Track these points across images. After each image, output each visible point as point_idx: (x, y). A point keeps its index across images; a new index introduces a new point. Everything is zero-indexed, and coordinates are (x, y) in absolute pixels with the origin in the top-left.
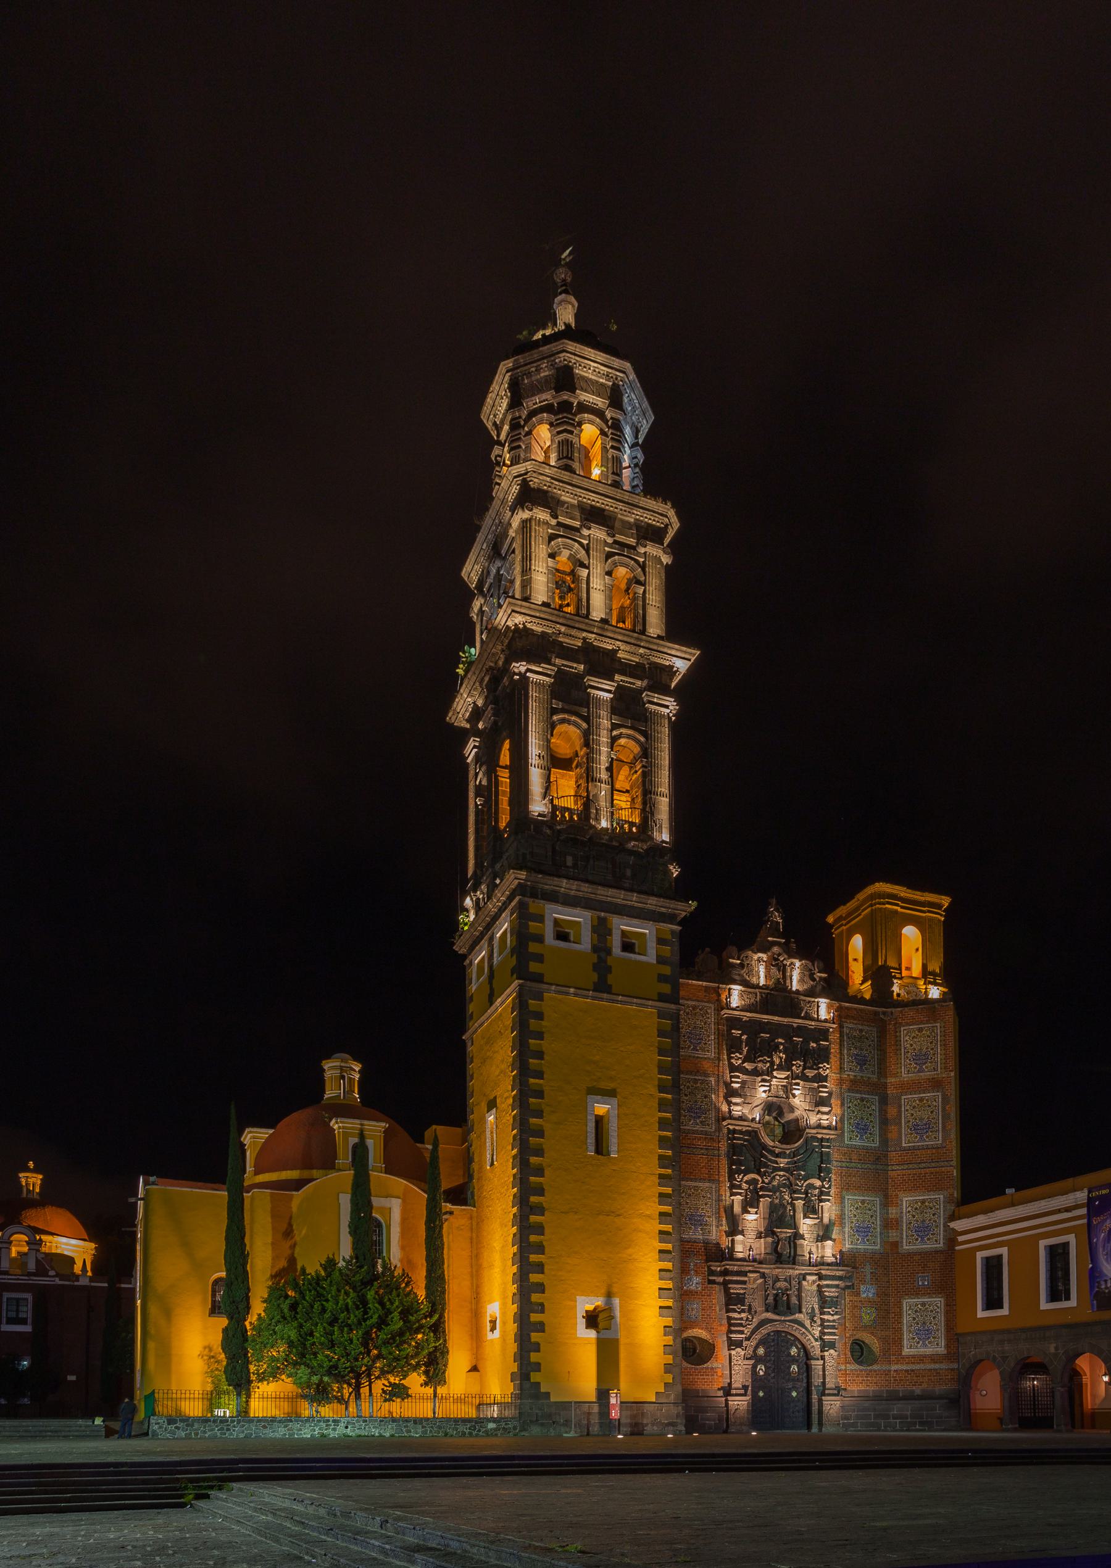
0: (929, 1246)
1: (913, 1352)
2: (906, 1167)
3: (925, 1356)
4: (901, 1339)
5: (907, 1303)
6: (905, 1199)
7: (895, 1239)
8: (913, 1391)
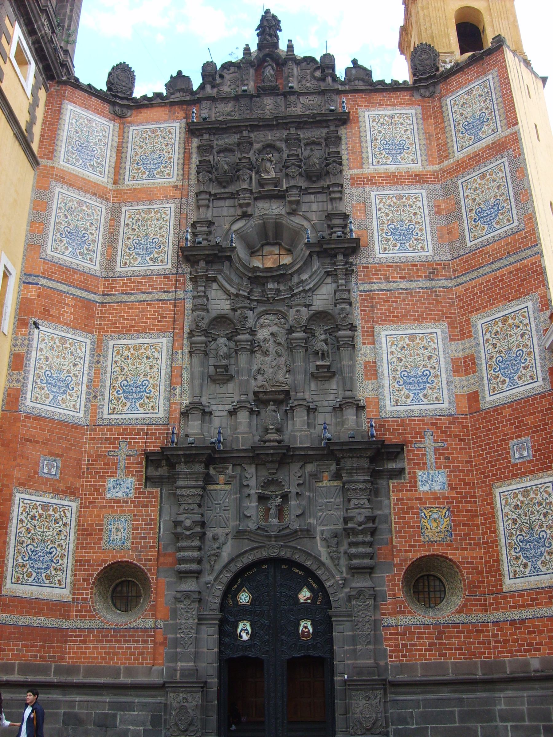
0: (522, 389)
1: (520, 584)
2: (475, 274)
3: (539, 591)
4: (498, 561)
6: (479, 323)
7: (473, 389)
8: (527, 664)
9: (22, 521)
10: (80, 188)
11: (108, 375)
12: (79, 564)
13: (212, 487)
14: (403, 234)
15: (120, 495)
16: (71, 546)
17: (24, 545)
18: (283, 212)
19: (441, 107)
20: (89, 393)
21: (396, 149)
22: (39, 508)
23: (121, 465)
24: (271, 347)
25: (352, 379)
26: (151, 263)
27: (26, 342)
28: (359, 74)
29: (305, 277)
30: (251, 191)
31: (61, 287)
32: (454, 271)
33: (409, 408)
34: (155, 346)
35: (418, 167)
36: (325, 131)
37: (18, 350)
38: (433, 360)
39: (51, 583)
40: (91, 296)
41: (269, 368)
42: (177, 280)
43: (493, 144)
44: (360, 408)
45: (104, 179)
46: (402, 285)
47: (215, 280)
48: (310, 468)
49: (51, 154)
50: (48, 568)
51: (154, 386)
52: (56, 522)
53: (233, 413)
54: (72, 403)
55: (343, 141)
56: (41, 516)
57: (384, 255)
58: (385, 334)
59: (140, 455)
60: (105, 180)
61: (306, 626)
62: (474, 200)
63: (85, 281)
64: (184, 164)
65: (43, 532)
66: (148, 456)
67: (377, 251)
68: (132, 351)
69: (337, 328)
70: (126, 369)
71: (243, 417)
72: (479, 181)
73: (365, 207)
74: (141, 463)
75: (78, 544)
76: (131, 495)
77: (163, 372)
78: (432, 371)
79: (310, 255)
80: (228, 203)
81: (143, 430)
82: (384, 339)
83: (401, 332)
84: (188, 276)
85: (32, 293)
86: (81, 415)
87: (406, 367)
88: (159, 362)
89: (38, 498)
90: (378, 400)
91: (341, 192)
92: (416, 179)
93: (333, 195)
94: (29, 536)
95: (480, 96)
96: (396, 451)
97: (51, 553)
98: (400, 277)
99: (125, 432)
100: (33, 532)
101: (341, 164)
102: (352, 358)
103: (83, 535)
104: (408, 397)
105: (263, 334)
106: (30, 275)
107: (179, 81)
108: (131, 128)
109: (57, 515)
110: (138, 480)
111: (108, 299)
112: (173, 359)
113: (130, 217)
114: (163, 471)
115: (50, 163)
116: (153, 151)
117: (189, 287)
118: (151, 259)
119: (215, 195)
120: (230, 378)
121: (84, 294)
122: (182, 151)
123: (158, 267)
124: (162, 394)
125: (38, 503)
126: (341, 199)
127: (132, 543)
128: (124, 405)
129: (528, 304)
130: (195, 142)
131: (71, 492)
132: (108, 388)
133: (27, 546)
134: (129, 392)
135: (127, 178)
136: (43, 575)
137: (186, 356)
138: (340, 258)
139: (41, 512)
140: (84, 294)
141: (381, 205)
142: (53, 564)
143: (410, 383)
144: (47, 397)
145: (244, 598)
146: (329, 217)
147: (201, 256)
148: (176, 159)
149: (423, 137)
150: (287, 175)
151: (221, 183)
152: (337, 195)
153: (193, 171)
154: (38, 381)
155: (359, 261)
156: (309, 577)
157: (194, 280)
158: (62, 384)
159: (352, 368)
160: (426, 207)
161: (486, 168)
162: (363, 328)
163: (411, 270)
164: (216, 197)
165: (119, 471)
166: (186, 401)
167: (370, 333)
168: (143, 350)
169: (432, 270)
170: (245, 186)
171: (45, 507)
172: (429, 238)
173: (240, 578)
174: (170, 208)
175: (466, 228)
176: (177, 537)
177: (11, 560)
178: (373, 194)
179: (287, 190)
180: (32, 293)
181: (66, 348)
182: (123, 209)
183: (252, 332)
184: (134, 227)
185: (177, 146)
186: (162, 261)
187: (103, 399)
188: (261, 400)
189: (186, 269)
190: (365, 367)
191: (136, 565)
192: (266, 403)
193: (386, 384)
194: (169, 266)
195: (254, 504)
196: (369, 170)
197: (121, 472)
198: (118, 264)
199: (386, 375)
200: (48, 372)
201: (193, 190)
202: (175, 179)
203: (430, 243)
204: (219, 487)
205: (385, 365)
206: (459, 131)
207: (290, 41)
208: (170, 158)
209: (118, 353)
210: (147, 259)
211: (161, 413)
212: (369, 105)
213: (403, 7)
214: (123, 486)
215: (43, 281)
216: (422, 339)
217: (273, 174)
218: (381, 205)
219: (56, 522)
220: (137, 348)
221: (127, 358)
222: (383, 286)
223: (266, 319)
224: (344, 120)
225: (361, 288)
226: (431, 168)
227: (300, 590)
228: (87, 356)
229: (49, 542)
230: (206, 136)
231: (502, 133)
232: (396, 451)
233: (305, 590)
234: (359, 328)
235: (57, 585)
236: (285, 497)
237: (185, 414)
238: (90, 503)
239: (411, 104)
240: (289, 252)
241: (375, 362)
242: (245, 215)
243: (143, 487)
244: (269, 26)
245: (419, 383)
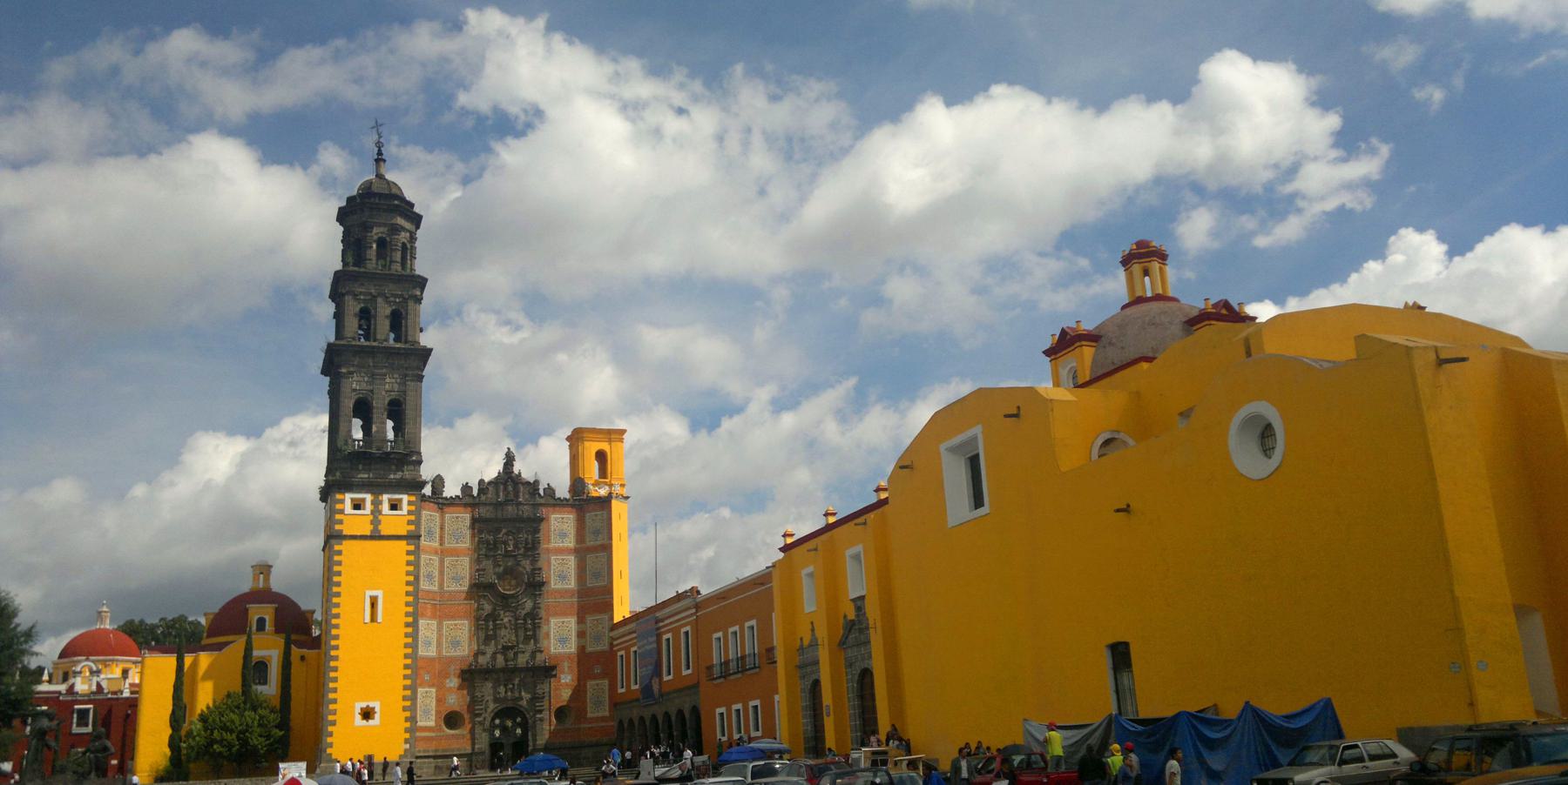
5: (590, 684)
14: (563, 577)
28: (550, 491)
41: (507, 636)
45: (436, 544)
61: (519, 731)
96: (554, 668)
99: (451, 660)
107: (466, 488)
123: (459, 588)
129: (606, 617)
131: (432, 686)
173: (497, 715)
196: (552, 545)
214: (453, 682)
224: (541, 520)
231: (606, 542)
232: (554, 668)
237: (476, 655)
244: (509, 460)
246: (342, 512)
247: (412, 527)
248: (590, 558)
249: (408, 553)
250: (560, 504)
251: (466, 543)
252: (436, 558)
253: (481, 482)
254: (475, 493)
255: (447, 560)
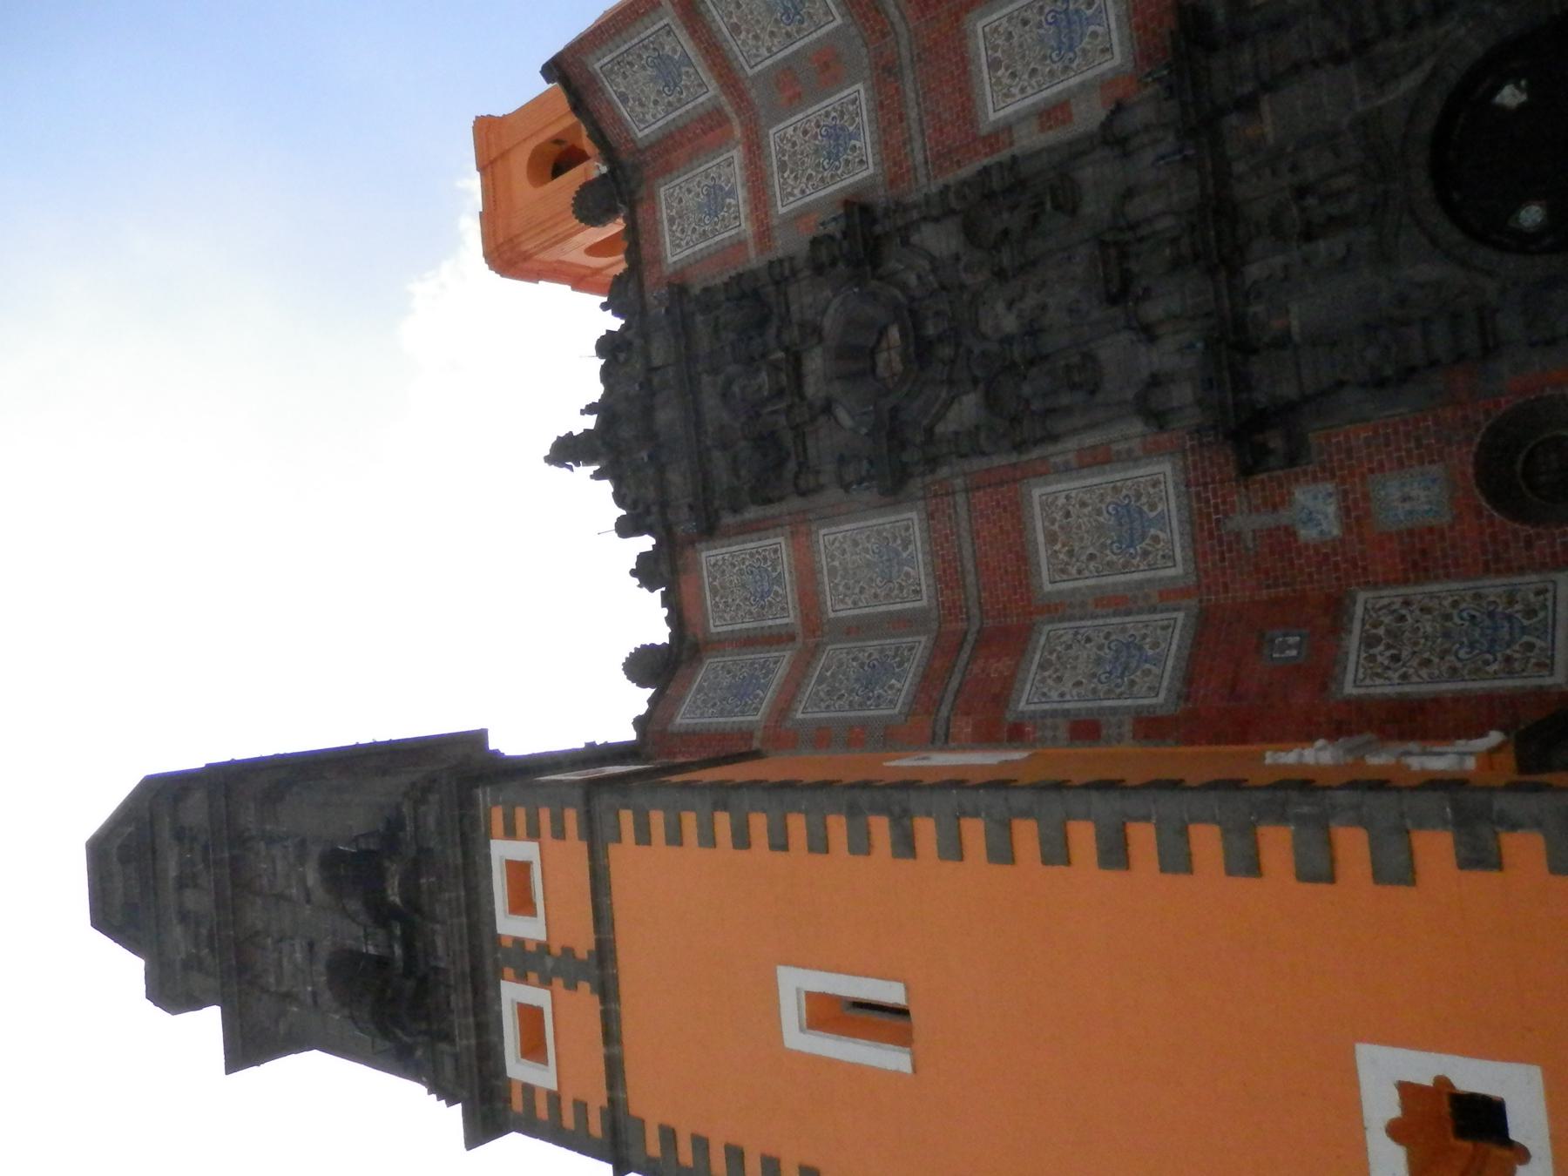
9: (1404, 677)
10: (798, 685)
11: (1104, 581)
12: (1496, 564)
13: (1297, 338)
15: (1331, 509)
16: (1455, 586)
17: (1459, 665)
18: (818, 351)
19: (651, 146)
20: (1140, 611)
21: (716, 197)
22: (1372, 651)
23: (1266, 520)
24: (1031, 301)
25: (1070, 144)
26: (911, 547)
27: (1049, 721)
29: (913, 280)
30: (790, 407)
31: (954, 683)
32: (884, 35)
33: (1113, 26)
34: (1044, 506)
35: (737, 154)
36: (699, 318)
37: (1063, 733)
38: (1028, 15)
39: (1544, 607)
40: (971, 638)
42: (935, 496)
43: (687, 28)
44: (1119, 108)
46: (913, 114)
47: (930, 431)
48: (1239, 167)
49: (746, 734)
50: (1509, 618)
51: (1116, 490)
52: (1402, 618)
53: (1149, 333)
54: (1159, 632)
55: (712, 283)
56: (1389, 647)
57: (870, 161)
58: (994, 110)
59: (1247, 487)
60: (788, 654)
62: (772, 34)
63: (946, 649)
64: (758, 530)
65: (1426, 638)
66: (1246, 471)
67: (865, 174)
68: (1057, 547)
69: (989, 196)
70: (1091, 550)
71: (1153, 311)
72: (743, 36)
73: (800, 215)
74: (1262, 482)
75: (1448, 576)
76: (1330, 487)
77: (1088, 482)
78: (1047, 10)
79: (880, 278)
80: (810, 443)
81: (1198, 494)
82: (1001, 113)
83: (988, 87)
84: (929, 479)
85: (964, 726)
86: (1180, 616)
87: (1045, 57)
88: (1073, 494)
89: (1353, 658)
90: (1105, 83)
91: (781, 261)
92: (755, 149)
93: (787, 272)
94: (1436, 660)
95: (625, 76)
97: (1473, 617)
98: (901, 120)
99: (1206, 529)
100: (1426, 655)
101: (740, 276)
102: (1037, 154)
103: (1426, 570)
104: (1094, 35)
105: (1010, 323)
106: (934, 733)
107: (646, 571)
108: (713, 630)
109: (1387, 620)
110: (1297, 480)
111: (975, 611)
112: (1066, 470)
113: (842, 601)
114: (1275, 441)
115: (759, 734)
116: (743, 586)
117: (944, 471)
118: (905, 548)
119: (800, 465)
120: (1089, 358)
121: (967, 648)
122: (741, 538)
123: (917, 533)
124: (1130, 474)
125: (1364, 655)
126: (791, 259)
127: (1432, 462)
128: (1156, 539)
130: (728, 519)
131: (1336, 608)
132: (1128, 577)
133: (1459, 659)
134: (1132, 535)
135: (786, 621)
136: (1526, 623)
137: (1060, 447)
138: (878, 229)
139: (1381, 648)
140: (967, 648)
141: (796, 192)
142: (1500, 609)
143: (1071, 39)
144: (1147, 673)
145: (1532, 215)
146: (818, 269)
147: (895, 462)
148: (752, 545)
149: (695, 163)
150: (763, 356)
151: (781, 464)
152: (786, 265)
153: (771, 510)
154: (1118, 691)
155: (880, 197)
156: (1468, 96)
157: (933, 463)
158: (1124, 654)
159: (1050, 150)
160: (794, 119)
161: (724, 29)
162: (986, 155)
163: (888, 111)
164: (803, 465)
165: (1285, 521)
166: (1137, 427)
167: (995, 139)
168: (1056, 527)
169: (886, 73)
170: (783, 421)
171: (1369, 641)
172: (838, 97)
174: (828, 538)
175: (815, 36)
176: (1408, 373)
177: (1497, 683)
178: (782, 210)
179: (787, 350)
180: (964, 726)
181: (1059, 658)
182: (832, 615)
183: (1007, 340)
184: (857, 590)
185: (734, 548)
186: (907, 529)
187: (1149, 581)
188: (1120, 291)
189: (915, 485)
190: (1050, 128)
191: (1481, 445)
192: (1127, 280)
193: (1074, 81)
194: (914, 515)
195: (1322, 245)
196: (746, 228)
197: (1285, 517)
198: (917, 604)
199: (1060, 87)
200: (1103, 678)
201: (795, 503)
202: (781, 539)
203: (846, 93)
204: (1295, 324)
205: (1044, 94)
206: (679, 100)
207: (583, 412)
208: (752, 555)
209: (1063, 571)
210: (905, 555)
211: (1164, 469)
212: (658, 260)
213: (544, 286)
214: (1315, 510)
215: (944, 711)
216: (995, 48)
217: (764, 377)
218: (796, 192)
219: (1402, 618)
220: (1051, 538)
221: (1071, 553)
222: (917, 145)
223: (986, 326)
224: (679, 289)
225: (923, 180)
226: (738, 133)
227: (1502, 109)
228: (1072, 624)
229: (1449, 624)
230: (717, 503)
233: (1498, 99)
234: (986, 161)
235: (1549, 595)
236: (1301, 192)
237: (1157, 418)
238: (1355, 566)
239: (652, 196)
240: (882, 332)
241: (1040, 115)
242: (827, 408)
243: (1310, 468)
244: (566, 451)
245: (1069, 22)
246: (554, 1099)
247: (571, 817)
248: (757, 56)
249: (643, 837)
250: (635, 244)
251: (778, 544)
252: (834, 653)
253: (625, 528)
254: (646, 543)
255: (837, 608)
